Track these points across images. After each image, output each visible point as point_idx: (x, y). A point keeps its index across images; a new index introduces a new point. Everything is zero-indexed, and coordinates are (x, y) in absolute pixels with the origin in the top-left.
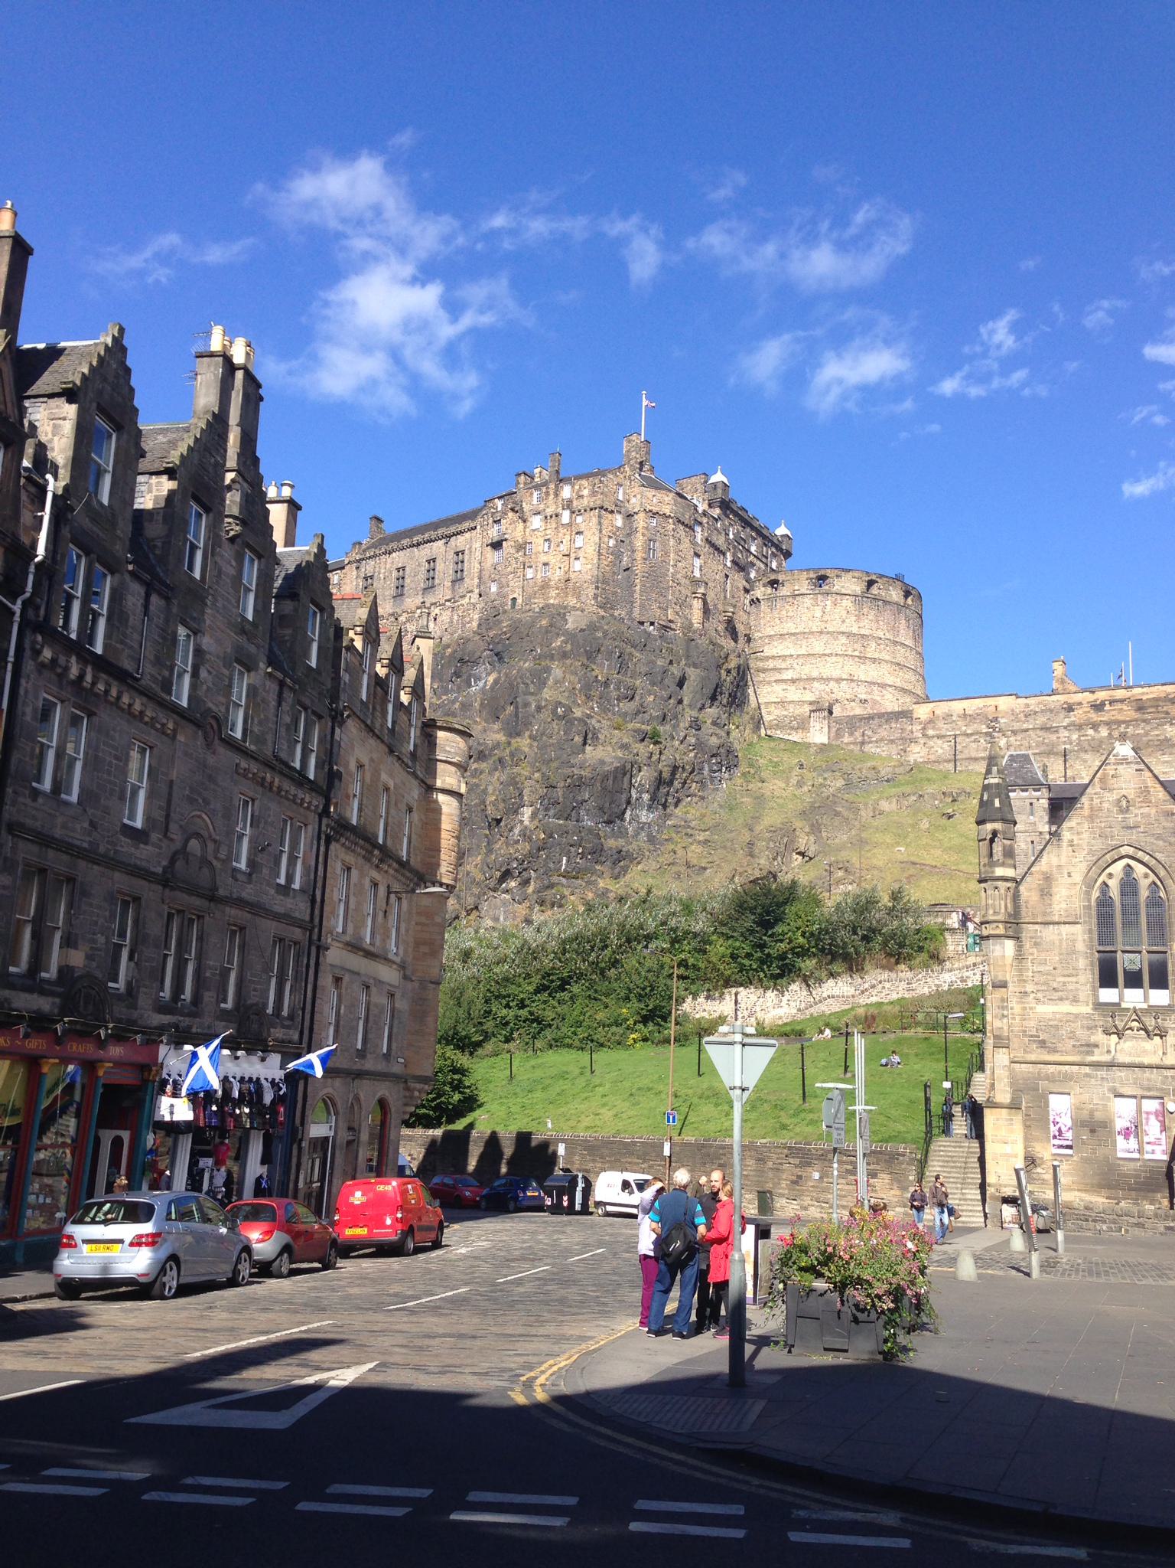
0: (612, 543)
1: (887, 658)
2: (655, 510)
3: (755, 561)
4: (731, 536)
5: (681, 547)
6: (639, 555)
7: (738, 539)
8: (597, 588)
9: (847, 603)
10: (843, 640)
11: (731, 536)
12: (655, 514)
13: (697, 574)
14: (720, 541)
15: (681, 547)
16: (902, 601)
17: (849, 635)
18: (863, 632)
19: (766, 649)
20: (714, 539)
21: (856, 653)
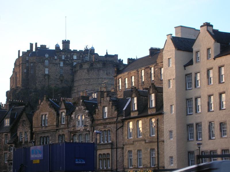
0: (25, 71)
1: (96, 83)
2: (32, 61)
3: (76, 61)
4: (63, 58)
5: (40, 68)
6: (30, 73)
7: (66, 58)
8: (22, 83)
9: (86, 71)
10: (84, 81)
11: (63, 58)
12: (32, 63)
13: (47, 72)
14: (57, 62)
15: (40, 68)
16: (101, 66)
17: (86, 79)
18: (89, 78)
19: (75, 85)
20: (54, 61)
21: (88, 84)
